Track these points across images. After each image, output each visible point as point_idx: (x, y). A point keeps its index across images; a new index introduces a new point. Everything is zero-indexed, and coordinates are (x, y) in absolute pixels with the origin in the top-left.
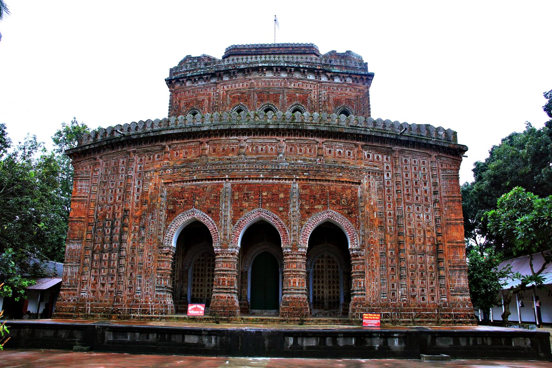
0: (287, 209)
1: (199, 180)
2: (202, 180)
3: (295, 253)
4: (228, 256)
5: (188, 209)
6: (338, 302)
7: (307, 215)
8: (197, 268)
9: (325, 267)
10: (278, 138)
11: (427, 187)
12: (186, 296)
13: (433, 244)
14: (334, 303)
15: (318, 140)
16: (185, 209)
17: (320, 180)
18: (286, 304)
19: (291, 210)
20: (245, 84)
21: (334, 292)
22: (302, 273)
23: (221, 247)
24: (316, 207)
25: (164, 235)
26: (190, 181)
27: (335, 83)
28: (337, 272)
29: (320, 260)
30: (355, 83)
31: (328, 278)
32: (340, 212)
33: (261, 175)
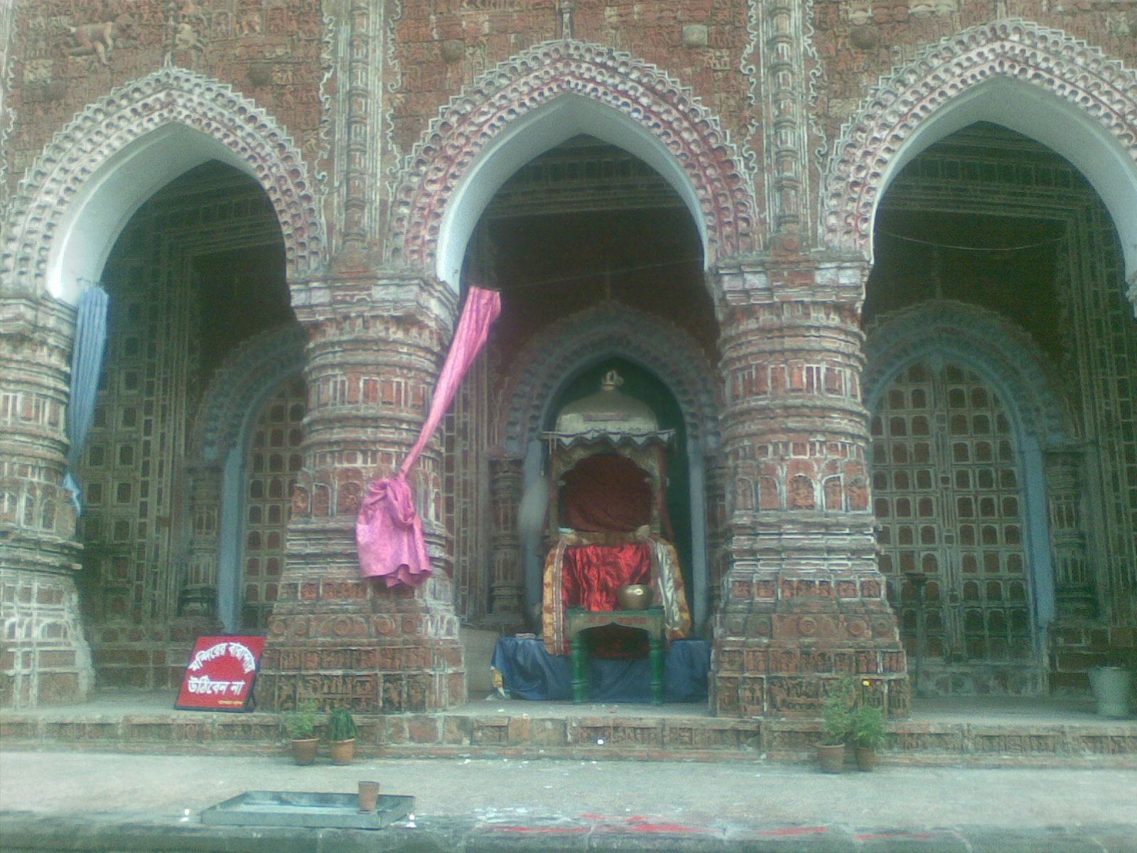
3: (795, 293)
4: (378, 330)
5: (139, 72)
6: (1020, 618)
7: (862, 60)
8: (268, 452)
9: (933, 424)
12: (210, 596)
14: (997, 621)
16: (118, 74)
18: (760, 621)
21: (992, 562)
22: (843, 424)
23: (330, 281)
28: (1006, 451)
29: (908, 391)
31: (953, 484)
32: (1079, 31)
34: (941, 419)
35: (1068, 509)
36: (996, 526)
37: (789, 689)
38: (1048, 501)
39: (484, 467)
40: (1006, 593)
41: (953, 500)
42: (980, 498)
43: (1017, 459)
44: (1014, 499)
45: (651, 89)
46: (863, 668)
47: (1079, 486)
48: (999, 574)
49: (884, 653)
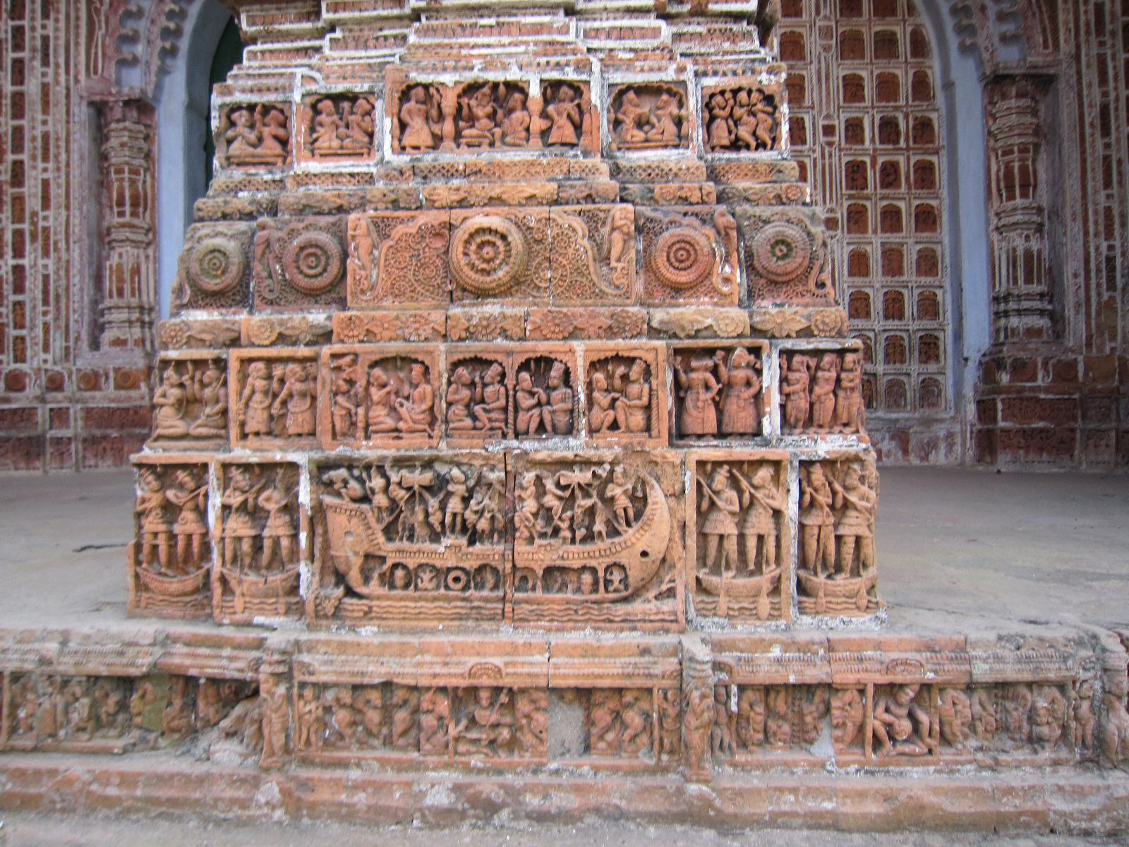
28: (921, 87)
31: (840, 136)
34: (826, 33)
35: (1023, 169)
36: (902, 205)
37: (394, 505)
38: (988, 159)
39: (81, 112)
40: (910, 307)
41: (839, 162)
42: (880, 160)
43: (940, 100)
44: (931, 164)
46: (702, 415)
47: (1043, 135)
48: (905, 278)
49: (788, 354)
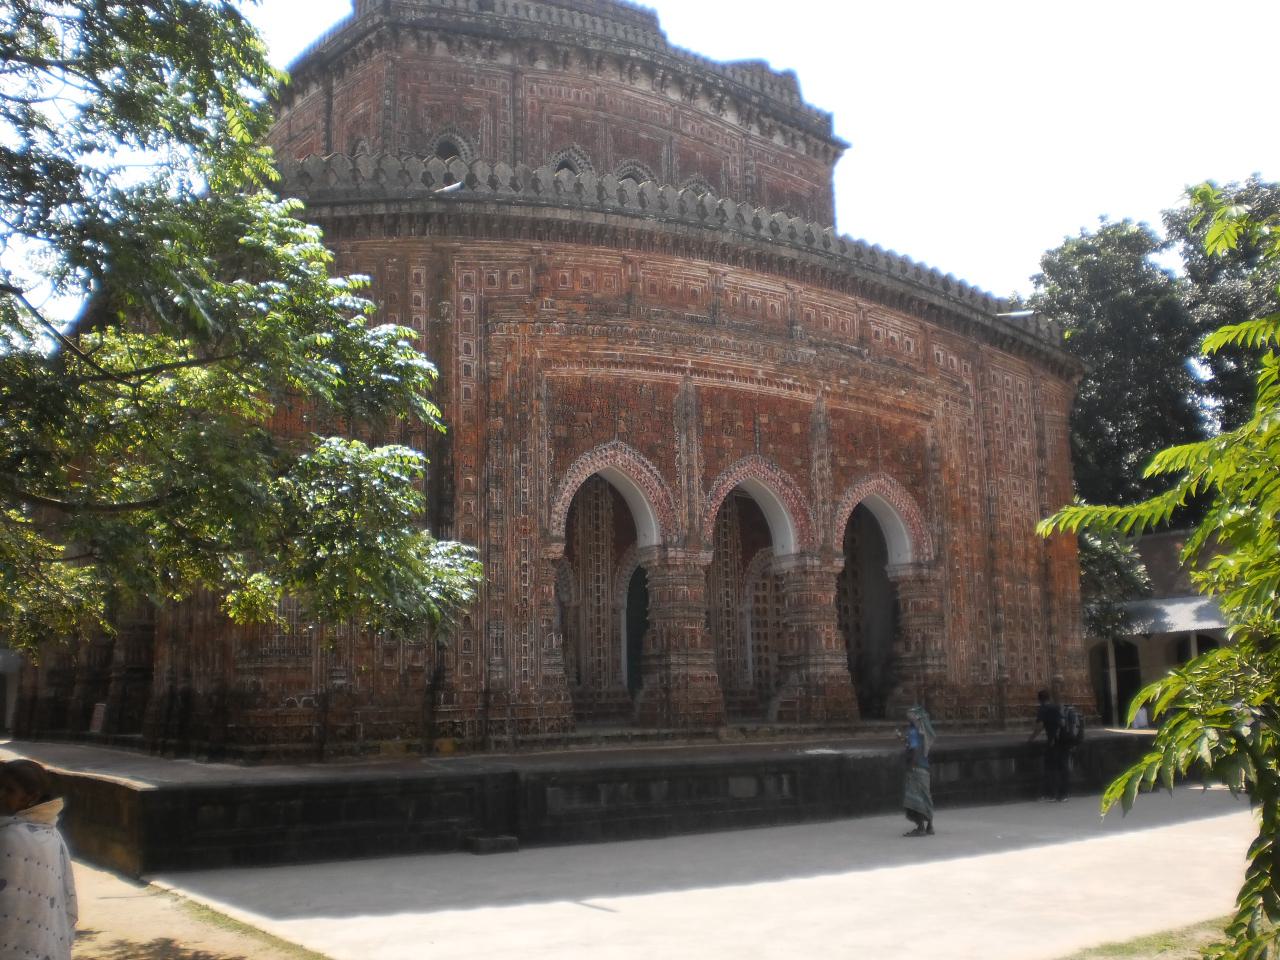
0: (807, 464)
1: (624, 365)
2: (631, 365)
10: (791, 284)
11: (1026, 443)
13: (1038, 562)
15: (862, 304)
17: (862, 399)
19: (816, 465)
20: (583, 93)
24: (859, 462)
25: (550, 508)
26: (602, 364)
27: (773, 145)
30: (811, 156)
33: (760, 372)
45: (783, 480)
